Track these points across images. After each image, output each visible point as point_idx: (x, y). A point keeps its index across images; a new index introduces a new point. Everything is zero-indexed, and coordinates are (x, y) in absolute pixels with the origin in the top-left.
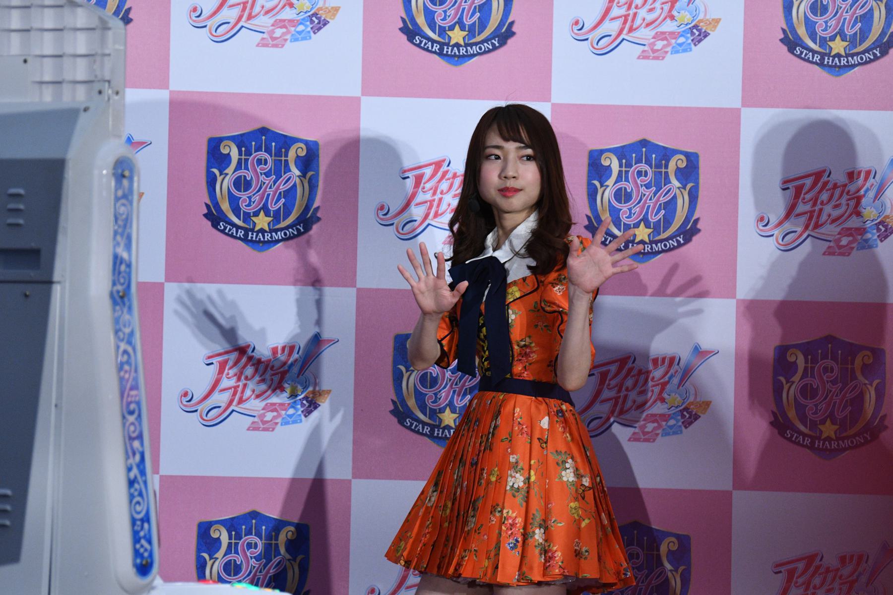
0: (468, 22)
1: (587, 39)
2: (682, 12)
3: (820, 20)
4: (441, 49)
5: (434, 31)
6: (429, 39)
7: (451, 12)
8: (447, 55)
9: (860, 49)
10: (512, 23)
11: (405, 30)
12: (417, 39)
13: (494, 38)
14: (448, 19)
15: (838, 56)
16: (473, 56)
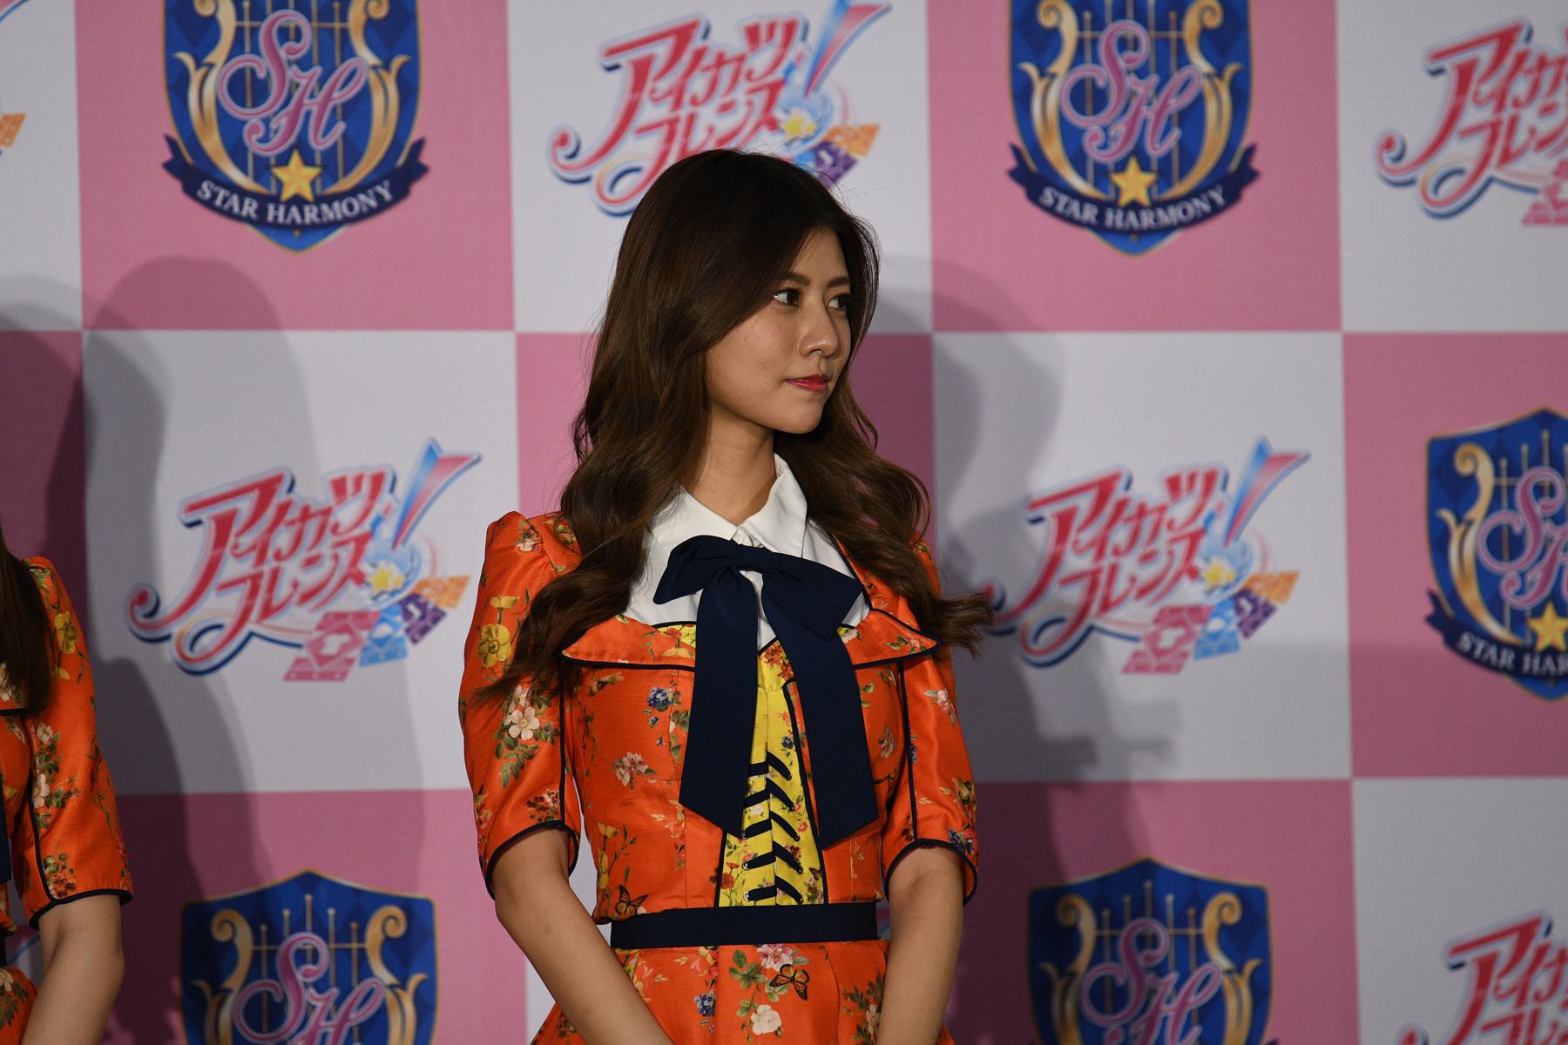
0: (319, 144)
1: (587, 180)
2: (794, 111)
3: (1091, 125)
4: (262, 211)
5: (242, 167)
6: (233, 188)
7: (281, 122)
8: (275, 225)
9: (1180, 189)
10: (419, 146)
11: (175, 167)
12: (206, 189)
13: (379, 182)
14: (275, 139)
15: (1135, 206)
16: (334, 225)
